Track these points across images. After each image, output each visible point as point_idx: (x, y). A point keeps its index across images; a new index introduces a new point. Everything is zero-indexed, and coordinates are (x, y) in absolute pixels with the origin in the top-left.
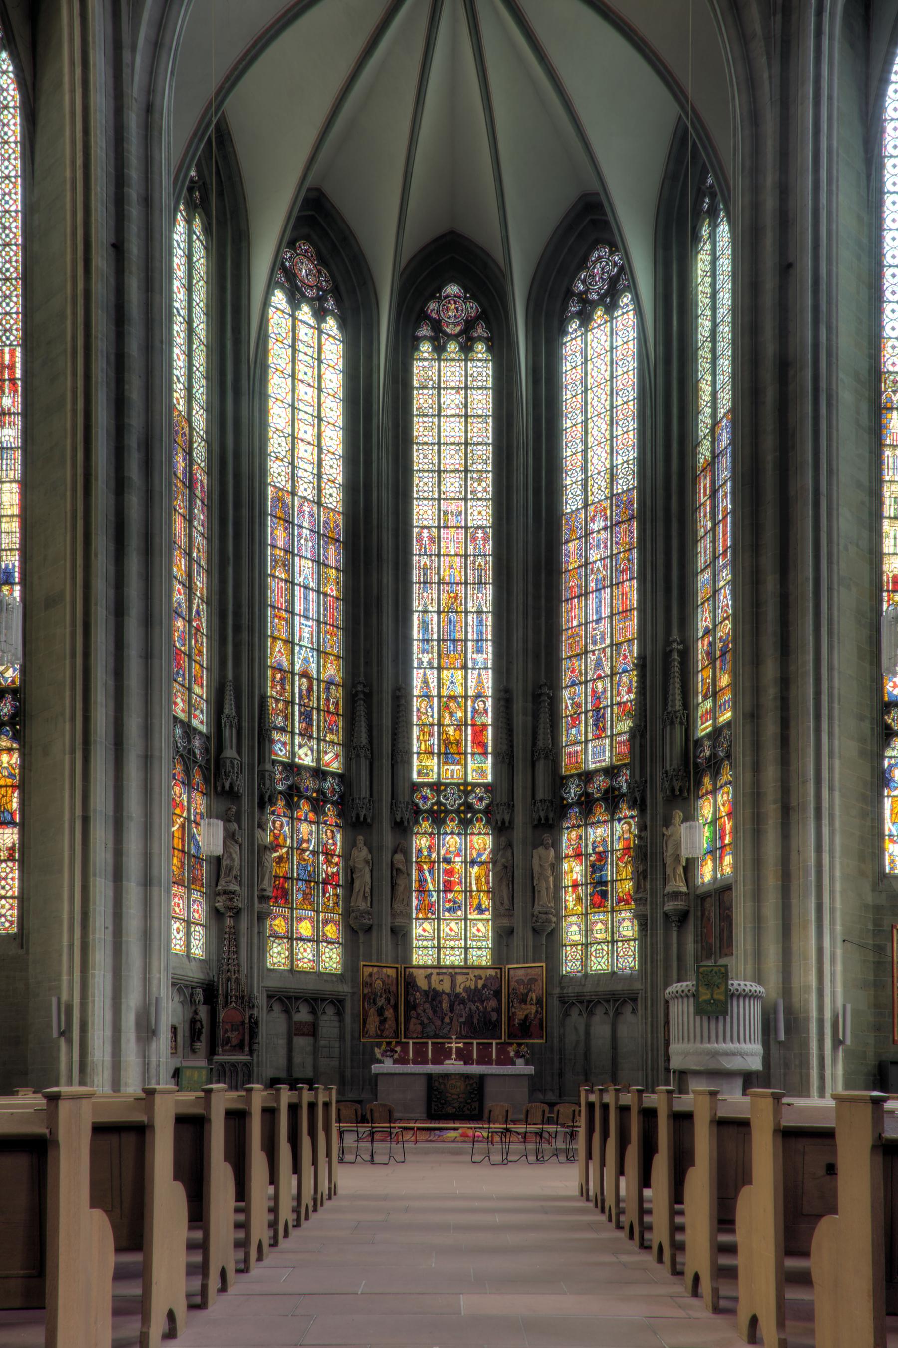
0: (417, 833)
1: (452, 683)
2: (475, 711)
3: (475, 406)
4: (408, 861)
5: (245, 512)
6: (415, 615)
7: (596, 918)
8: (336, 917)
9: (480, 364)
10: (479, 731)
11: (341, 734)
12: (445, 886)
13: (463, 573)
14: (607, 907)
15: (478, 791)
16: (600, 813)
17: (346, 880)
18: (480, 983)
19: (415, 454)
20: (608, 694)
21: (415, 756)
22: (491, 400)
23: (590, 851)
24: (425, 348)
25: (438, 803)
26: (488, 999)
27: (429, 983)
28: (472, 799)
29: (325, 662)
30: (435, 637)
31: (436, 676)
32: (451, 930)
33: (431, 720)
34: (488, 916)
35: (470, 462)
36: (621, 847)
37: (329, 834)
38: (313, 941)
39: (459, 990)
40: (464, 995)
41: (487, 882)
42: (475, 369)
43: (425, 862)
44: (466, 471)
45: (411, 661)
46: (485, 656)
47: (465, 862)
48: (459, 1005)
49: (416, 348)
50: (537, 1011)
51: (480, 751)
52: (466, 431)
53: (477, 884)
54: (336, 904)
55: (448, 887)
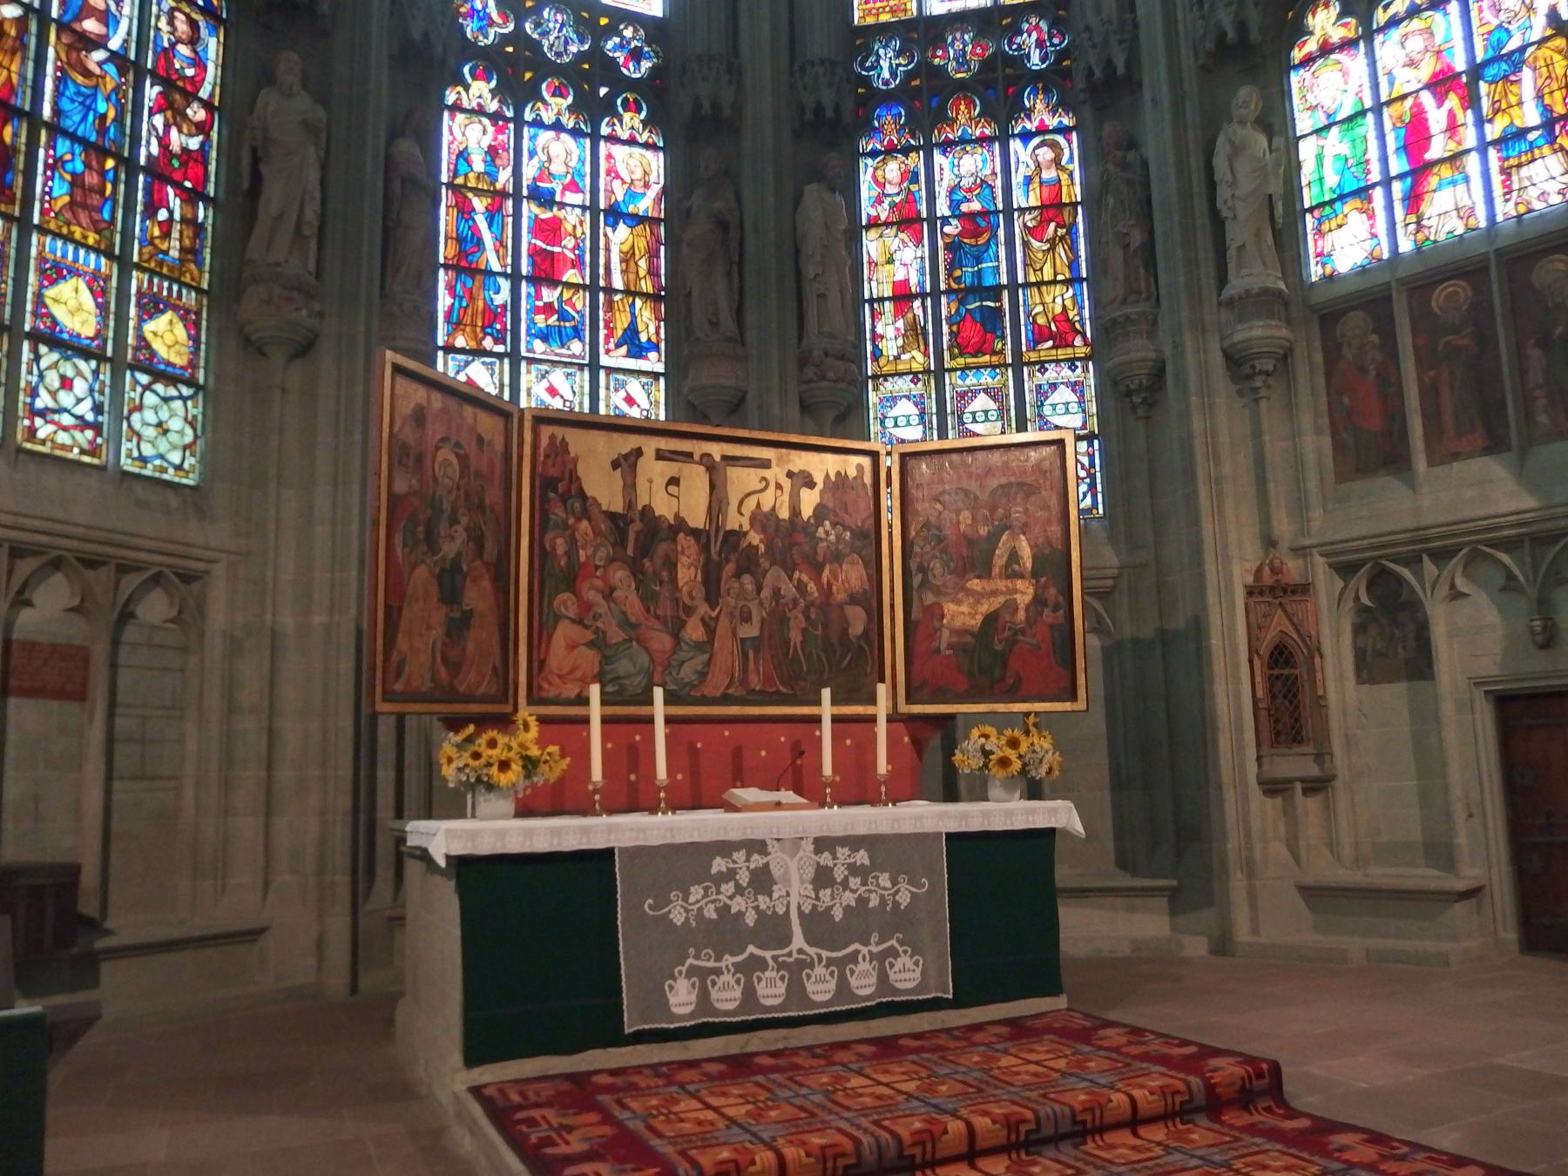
0: (457, 108)
8: (189, 298)
12: (534, 264)
14: (1001, 352)
15: (628, 33)
16: (966, 119)
23: (943, 209)
25: (518, 36)
32: (552, 391)
34: (654, 363)
36: (1034, 201)
38: (101, 358)
39: (735, 520)
41: (653, 272)
43: (478, 192)
47: (593, 208)
48: (738, 575)
53: (624, 272)
55: (546, 271)
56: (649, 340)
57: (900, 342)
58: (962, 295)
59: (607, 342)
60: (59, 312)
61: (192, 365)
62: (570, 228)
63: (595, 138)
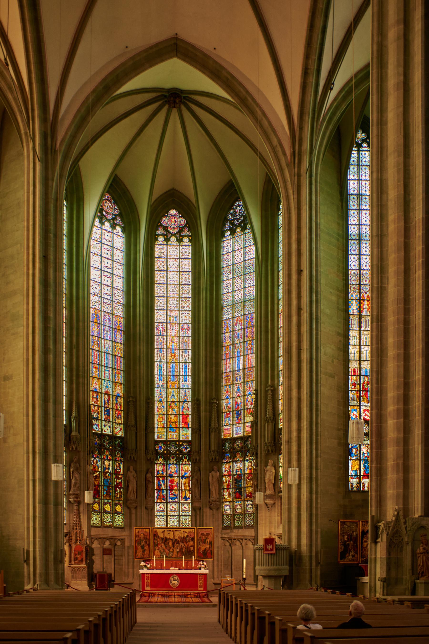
0: (157, 464)
1: (173, 395)
2: (183, 408)
3: (183, 267)
4: (153, 477)
5: (81, 324)
6: (156, 364)
7: (237, 503)
9: (185, 247)
10: (185, 417)
11: (122, 419)
12: (169, 487)
13: (178, 344)
14: (242, 498)
15: (184, 445)
17: (125, 485)
18: (186, 535)
19: (156, 289)
20: (243, 404)
21: (156, 428)
22: (190, 264)
23: (235, 473)
24: (161, 239)
25: (167, 450)
26: (189, 541)
27: (164, 535)
28: (182, 448)
29: (116, 386)
30: (165, 374)
31: (165, 392)
34: (189, 501)
35: (181, 293)
37: (118, 465)
38: (111, 513)
41: (189, 486)
42: (183, 250)
43: (160, 477)
44: (179, 297)
45: (154, 385)
46: (188, 383)
47: (179, 477)
49: (157, 239)
50: (210, 547)
51: (186, 426)
52: (179, 279)
54: (121, 496)
60: (106, 509)
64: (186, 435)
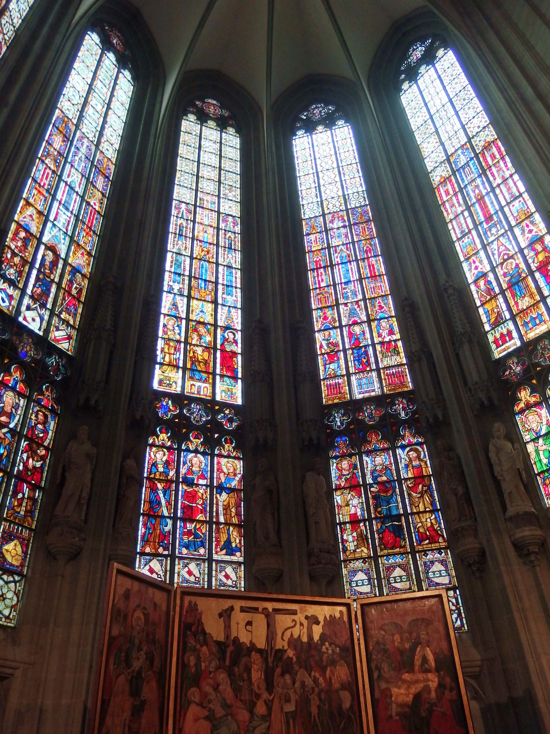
0: (153, 445)
1: (202, 311)
2: (225, 340)
8: (26, 533)
14: (405, 546)
15: (227, 412)
16: (375, 441)
23: (369, 480)
25: (180, 415)
32: (190, 573)
33: (178, 337)
34: (238, 557)
36: (410, 475)
37: (41, 417)
39: (281, 644)
40: (291, 653)
41: (238, 514)
43: (160, 481)
47: (210, 486)
48: (283, 675)
53: (225, 515)
55: (189, 515)
56: (236, 546)
57: (355, 543)
58: (383, 519)
59: (216, 547)
61: (22, 565)
62: (200, 495)
63: (212, 456)
64: (230, 391)
